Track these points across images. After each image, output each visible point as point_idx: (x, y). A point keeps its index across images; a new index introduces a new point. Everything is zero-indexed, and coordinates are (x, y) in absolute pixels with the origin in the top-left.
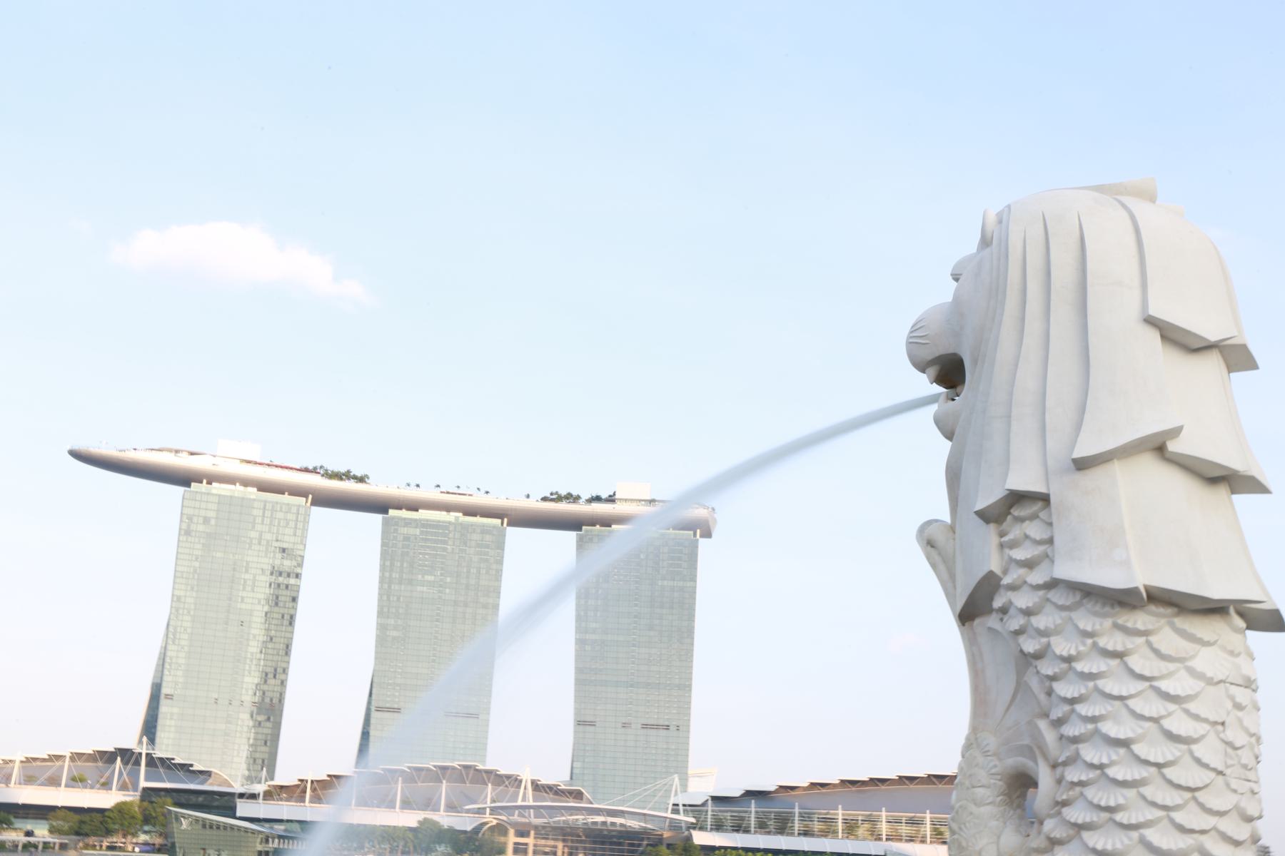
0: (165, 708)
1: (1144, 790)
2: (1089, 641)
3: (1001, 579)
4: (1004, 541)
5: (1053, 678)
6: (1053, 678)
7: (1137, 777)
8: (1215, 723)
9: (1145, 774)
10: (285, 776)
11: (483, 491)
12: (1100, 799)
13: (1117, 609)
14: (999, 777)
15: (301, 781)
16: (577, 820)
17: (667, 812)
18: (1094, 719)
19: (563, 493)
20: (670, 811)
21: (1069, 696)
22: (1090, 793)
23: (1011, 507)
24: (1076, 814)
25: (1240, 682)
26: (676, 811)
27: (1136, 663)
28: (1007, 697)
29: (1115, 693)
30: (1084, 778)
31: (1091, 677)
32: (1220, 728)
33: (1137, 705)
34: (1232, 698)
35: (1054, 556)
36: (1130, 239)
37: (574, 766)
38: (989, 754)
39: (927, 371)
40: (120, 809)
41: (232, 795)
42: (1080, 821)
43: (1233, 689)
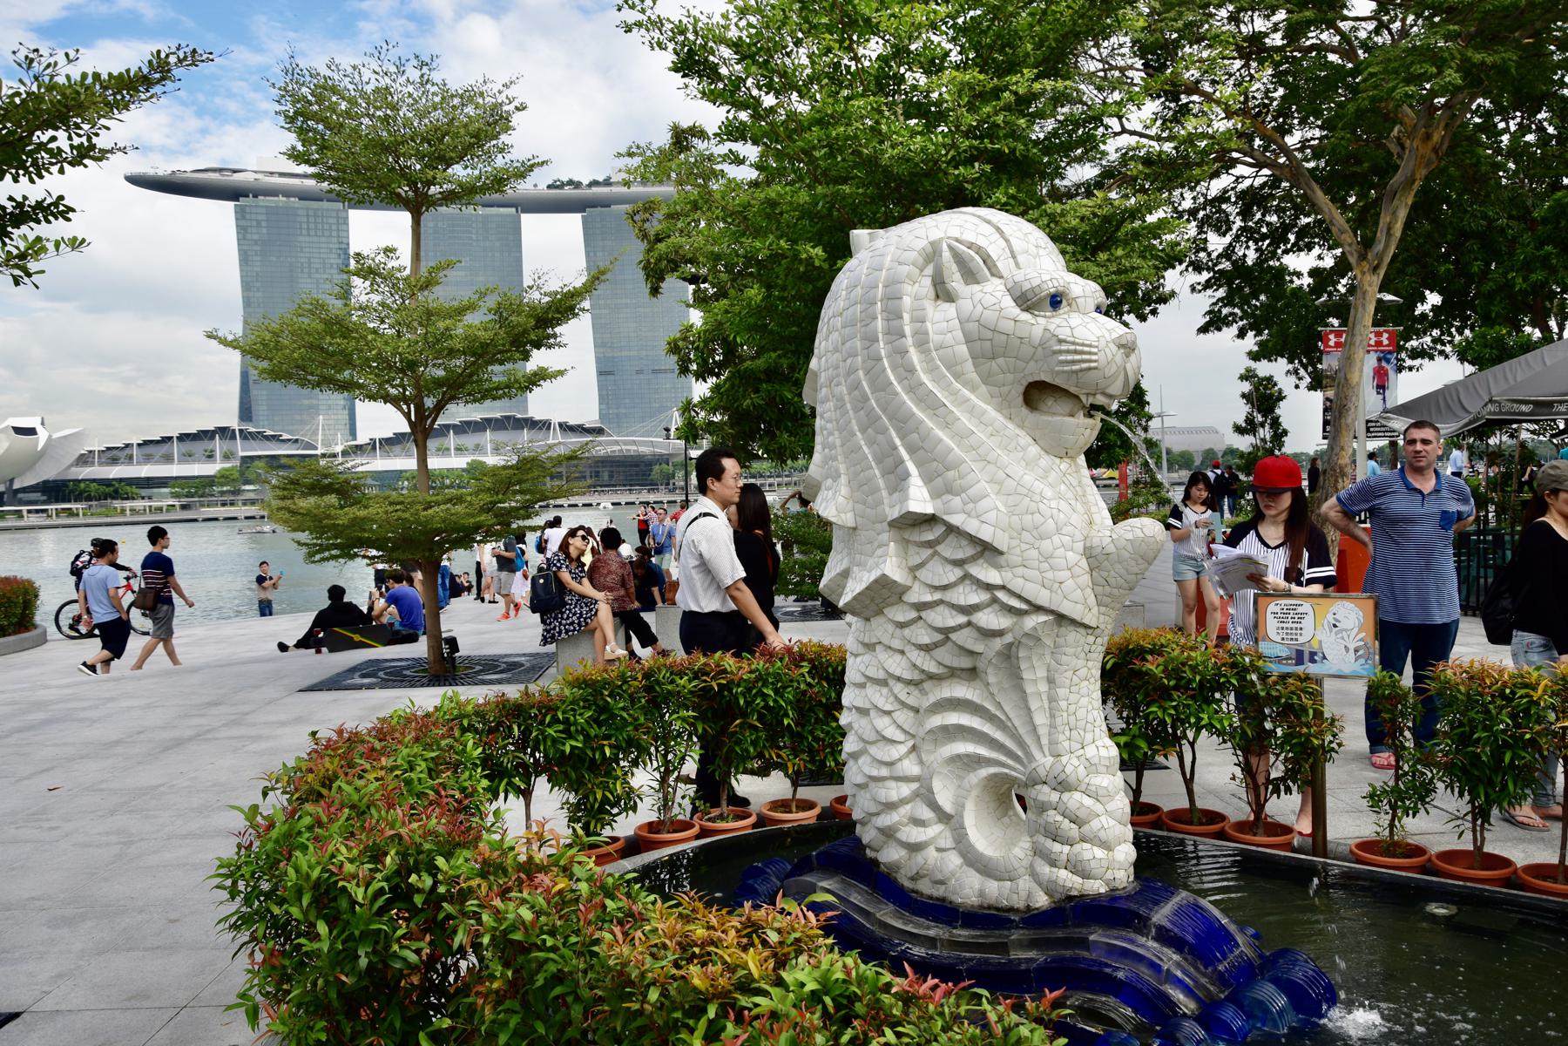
10: (362, 438)
19: (565, 179)
40: (223, 477)
41: (316, 455)
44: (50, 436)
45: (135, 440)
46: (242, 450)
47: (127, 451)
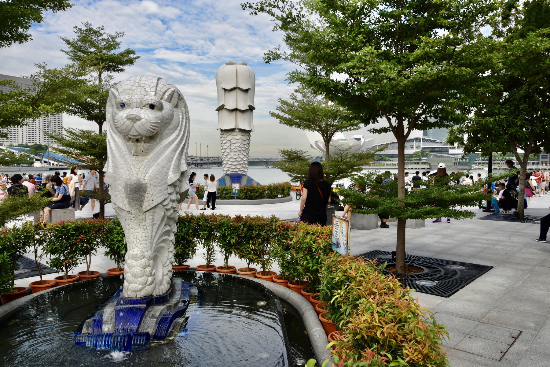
40: (416, 155)
44: (365, 141)
46: (423, 145)
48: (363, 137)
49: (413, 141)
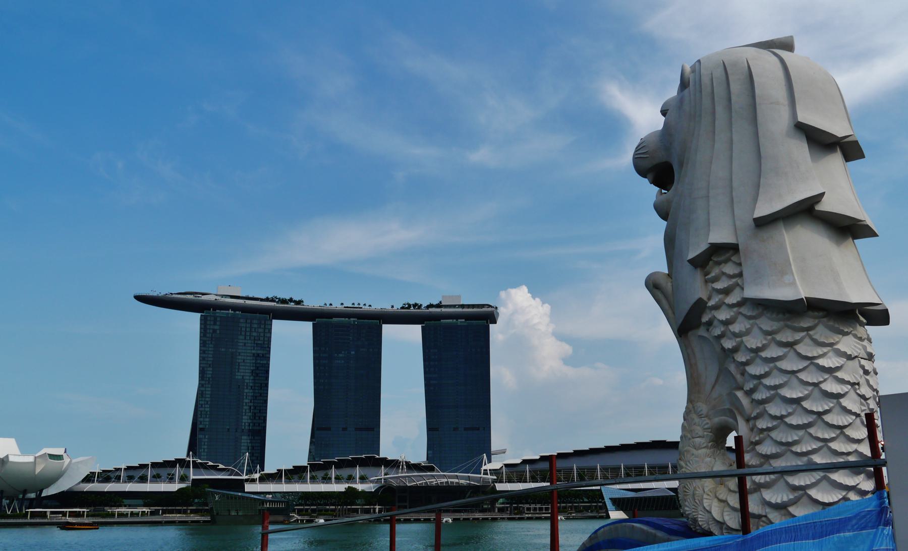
0: (200, 436)
1: (812, 431)
2: (769, 337)
3: (707, 303)
4: (708, 278)
5: (747, 363)
6: (747, 363)
7: (806, 422)
8: (853, 385)
9: (810, 420)
10: (270, 468)
11: (367, 305)
12: (782, 438)
13: (787, 315)
14: (710, 430)
15: (278, 470)
16: (433, 482)
17: (481, 474)
18: (776, 387)
20: (482, 474)
21: (758, 374)
22: (774, 434)
23: (711, 256)
24: (766, 448)
25: (866, 357)
26: (487, 474)
27: (802, 349)
28: (712, 379)
29: (789, 369)
30: (770, 425)
31: (773, 360)
32: (857, 387)
33: (803, 376)
34: (863, 367)
35: (743, 284)
36: (780, 73)
37: (429, 453)
38: (703, 416)
39: (648, 176)
42: (769, 453)
43: (863, 362)
45: (123, 466)
47: (118, 474)
48: (65, 452)
49: (176, 466)
